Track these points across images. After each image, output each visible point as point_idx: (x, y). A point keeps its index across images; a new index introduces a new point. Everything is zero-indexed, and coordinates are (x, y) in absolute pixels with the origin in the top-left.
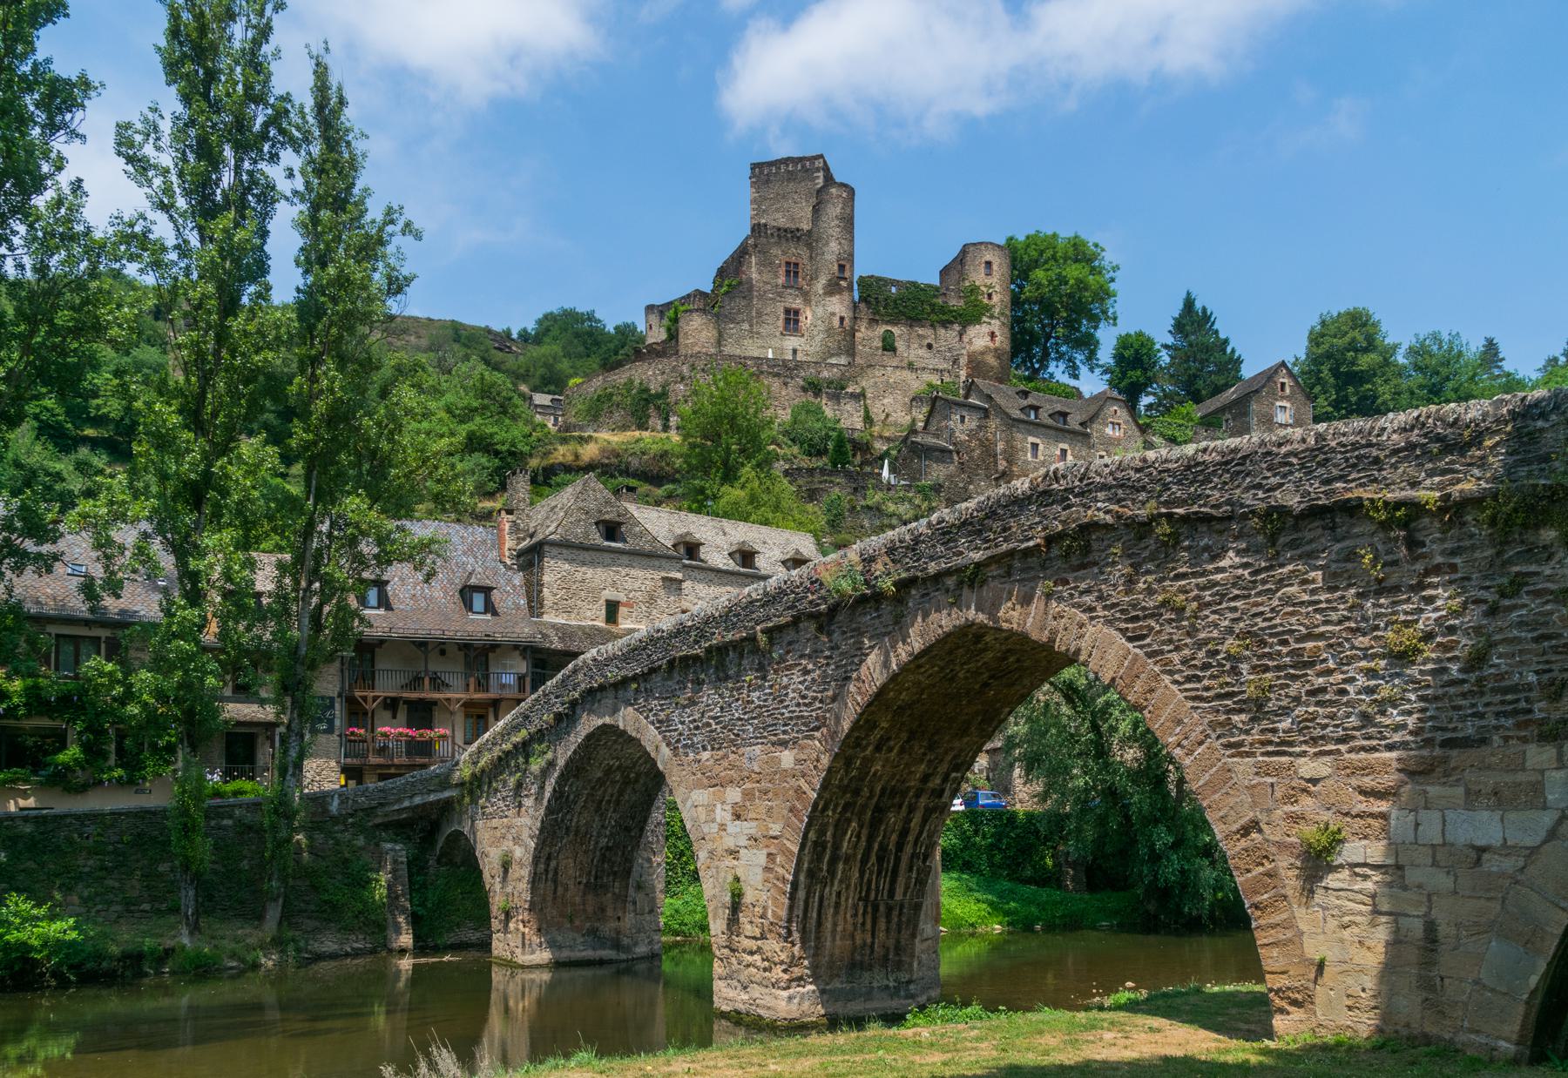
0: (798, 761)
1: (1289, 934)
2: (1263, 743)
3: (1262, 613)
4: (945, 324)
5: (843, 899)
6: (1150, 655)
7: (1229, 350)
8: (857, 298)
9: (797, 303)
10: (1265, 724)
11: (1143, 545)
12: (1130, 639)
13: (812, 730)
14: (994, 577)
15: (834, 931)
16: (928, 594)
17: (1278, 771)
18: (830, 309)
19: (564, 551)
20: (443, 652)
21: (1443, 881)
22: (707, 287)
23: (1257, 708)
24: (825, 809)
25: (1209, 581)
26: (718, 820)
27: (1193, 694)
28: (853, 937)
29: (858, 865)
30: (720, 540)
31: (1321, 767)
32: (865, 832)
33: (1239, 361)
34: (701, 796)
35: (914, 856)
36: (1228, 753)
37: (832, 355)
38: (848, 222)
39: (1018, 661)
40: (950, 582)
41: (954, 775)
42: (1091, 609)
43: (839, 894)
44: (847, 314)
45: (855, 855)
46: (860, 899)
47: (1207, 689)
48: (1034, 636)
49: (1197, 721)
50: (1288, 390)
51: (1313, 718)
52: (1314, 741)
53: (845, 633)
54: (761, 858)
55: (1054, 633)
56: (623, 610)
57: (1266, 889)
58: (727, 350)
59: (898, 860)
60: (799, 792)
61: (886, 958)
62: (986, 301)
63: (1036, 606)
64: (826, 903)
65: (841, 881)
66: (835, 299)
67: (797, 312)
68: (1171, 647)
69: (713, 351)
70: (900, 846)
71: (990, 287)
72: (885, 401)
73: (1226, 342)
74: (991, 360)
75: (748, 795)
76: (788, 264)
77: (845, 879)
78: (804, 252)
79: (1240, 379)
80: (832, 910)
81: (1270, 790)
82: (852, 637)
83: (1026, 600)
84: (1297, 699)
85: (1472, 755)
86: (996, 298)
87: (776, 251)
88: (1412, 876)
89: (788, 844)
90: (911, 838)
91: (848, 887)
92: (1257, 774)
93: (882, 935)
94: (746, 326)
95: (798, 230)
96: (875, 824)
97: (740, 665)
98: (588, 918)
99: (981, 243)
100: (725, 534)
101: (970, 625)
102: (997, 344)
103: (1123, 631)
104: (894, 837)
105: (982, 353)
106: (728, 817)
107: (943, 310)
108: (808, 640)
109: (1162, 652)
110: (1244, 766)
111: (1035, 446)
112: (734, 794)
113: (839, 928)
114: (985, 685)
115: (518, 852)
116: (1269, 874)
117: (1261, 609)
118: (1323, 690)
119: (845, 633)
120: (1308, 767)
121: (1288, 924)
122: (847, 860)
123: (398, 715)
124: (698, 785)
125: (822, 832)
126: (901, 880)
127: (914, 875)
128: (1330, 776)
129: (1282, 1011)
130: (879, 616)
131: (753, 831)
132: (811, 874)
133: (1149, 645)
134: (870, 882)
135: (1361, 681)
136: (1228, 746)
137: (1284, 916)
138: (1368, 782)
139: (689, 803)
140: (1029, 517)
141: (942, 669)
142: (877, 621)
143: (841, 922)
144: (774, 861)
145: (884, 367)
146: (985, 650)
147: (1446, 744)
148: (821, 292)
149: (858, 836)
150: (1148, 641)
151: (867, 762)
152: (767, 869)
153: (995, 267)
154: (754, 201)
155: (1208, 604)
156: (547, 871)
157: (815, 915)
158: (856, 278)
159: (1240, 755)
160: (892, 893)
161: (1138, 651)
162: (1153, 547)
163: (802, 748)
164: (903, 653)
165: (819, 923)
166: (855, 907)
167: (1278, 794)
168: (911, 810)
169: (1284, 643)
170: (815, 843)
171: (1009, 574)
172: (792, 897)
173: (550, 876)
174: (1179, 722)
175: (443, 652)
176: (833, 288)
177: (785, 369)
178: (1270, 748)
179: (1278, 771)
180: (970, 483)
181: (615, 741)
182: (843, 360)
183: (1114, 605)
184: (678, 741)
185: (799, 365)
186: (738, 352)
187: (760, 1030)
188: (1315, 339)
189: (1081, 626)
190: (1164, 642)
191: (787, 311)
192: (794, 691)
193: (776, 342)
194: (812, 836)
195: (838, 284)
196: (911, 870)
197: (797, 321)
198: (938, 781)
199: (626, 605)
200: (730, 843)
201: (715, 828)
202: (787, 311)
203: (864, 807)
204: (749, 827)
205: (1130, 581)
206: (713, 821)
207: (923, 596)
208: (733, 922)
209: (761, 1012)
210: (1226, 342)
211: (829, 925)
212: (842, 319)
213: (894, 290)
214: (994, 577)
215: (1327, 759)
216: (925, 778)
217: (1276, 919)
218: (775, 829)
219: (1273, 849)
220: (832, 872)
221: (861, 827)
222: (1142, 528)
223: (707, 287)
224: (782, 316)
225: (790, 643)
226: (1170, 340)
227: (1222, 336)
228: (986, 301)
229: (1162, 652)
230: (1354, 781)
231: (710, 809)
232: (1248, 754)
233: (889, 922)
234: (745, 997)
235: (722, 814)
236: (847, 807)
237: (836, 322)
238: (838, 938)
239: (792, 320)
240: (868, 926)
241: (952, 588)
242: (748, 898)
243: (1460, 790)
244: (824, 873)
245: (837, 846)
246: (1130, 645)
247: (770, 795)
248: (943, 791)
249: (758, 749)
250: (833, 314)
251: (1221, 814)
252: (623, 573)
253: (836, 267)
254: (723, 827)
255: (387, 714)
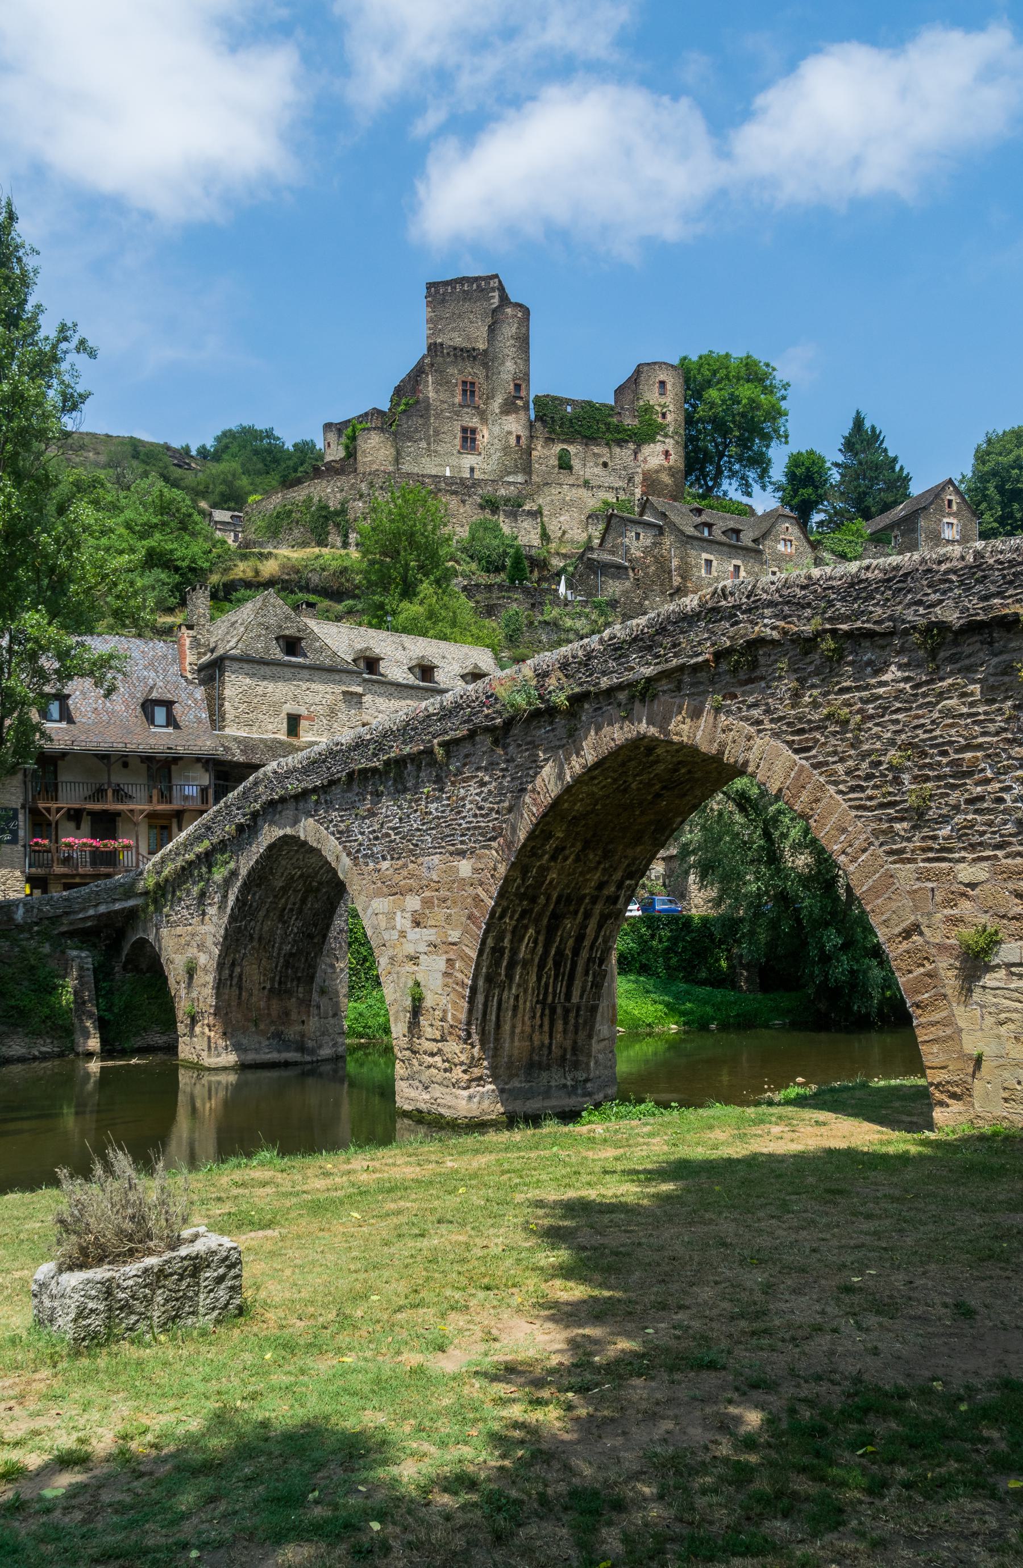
0: (476, 870)
1: (949, 1031)
2: (924, 850)
3: (923, 725)
4: (620, 443)
5: (521, 1002)
6: (815, 766)
7: (897, 468)
8: (533, 417)
9: (474, 422)
10: (926, 832)
11: (808, 660)
12: (796, 751)
13: (489, 840)
14: (664, 692)
15: (513, 1033)
16: (600, 708)
17: (938, 876)
18: (506, 428)
19: (245, 666)
20: (125, 765)
22: (386, 406)
23: (918, 817)
24: (502, 917)
25: (872, 695)
26: (398, 927)
27: (857, 803)
28: (531, 1039)
29: (535, 970)
30: (400, 655)
31: (979, 872)
32: (541, 938)
33: (907, 479)
34: (381, 904)
35: (590, 960)
36: (890, 859)
37: (509, 474)
38: (523, 342)
39: (689, 772)
40: (622, 696)
41: (628, 882)
42: (758, 722)
43: (517, 997)
44: (524, 433)
45: (532, 959)
46: (537, 1002)
47: (870, 798)
48: (704, 748)
49: (860, 829)
50: (955, 507)
51: (972, 826)
52: (973, 847)
53: (520, 746)
54: (440, 964)
55: (723, 745)
56: (304, 724)
57: (927, 988)
58: (405, 468)
59: (574, 965)
60: (477, 900)
61: (563, 1058)
62: (660, 420)
63: (705, 720)
64: (504, 1005)
65: (519, 986)
66: (511, 418)
67: (474, 431)
68: (836, 759)
69: (391, 468)
70: (576, 952)
71: (664, 406)
72: (562, 519)
73: (895, 460)
74: (666, 479)
75: (427, 903)
76: (464, 383)
77: (524, 982)
78: (480, 372)
79: (907, 496)
80: (510, 1013)
81: (930, 894)
82: (527, 750)
83: (696, 714)
84: (956, 808)
86: (670, 418)
87: (452, 370)
89: (467, 950)
90: (587, 943)
91: (525, 991)
92: (918, 879)
93: (558, 1037)
94: (423, 444)
95: (474, 349)
96: (551, 931)
97: (418, 777)
98: (273, 1022)
99: (655, 363)
100: (404, 649)
101: (641, 738)
102: (671, 463)
103: (791, 744)
104: (571, 942)
105: (657, 472)
106: (408, 924)
107: (618, 429)
108: (484, 753)
109: (827, 763)
110: (905, 872)
111: (709, 562)
112: (413, 902)
113: (518, 1030)
114: (658, 796)
115: (203, 959)
116: (929, 975)
117: (922, 721)
118: (981, 798)
119: (520, 746)
120: (966, 872)
121: (948, 1022)
122: (525, 964)
123: (83, 826)
124: (378, 894)
125: (500, 938)
126: (578, 984)
127: (590, 979)
128: (988, 880)
129: (942, 1104)
130: (553, 730)
131: (432, 938)
132: (489, 979)
133: (815, 757)
134: (547, 985)
136: (890, 853)
137: (944, 1014)
139: (370, 911)
140: (698, 633)
141: (615, 780)
142: (551, 734)
143: (519, 1025)
144: (453, 966)
145: (561, 485)
146: (657, 762)
148: (497, 411)
149: (536, 942)
150: (814, 752)
151: (544, 870)
152: (446, 974)
153: (669, 387)
154: (430, 321)
155: (871, 717)
156: (231, 976)
157: (494, 1018)
158: (532, 398)
159: (902, 861)
160: (568, 996)
161: (804, 762)
162: (818, 662)
163: (480, 857)
164: (576, 765)
165: (498, 1025)
166: (533, 1010)
167: (938, 899)
168: (587, 915)
169: (944, 753)
170: (494, 950)
171: (679, 689)
172: (471, 1001)
173: (235, 981)
174: (844, 830)
175: (125, 765)
176: (509, 407)
177: (463, 487)
178: (931, 855)
179: (938, 876)
180: (646, 598)
181: (297, 851)
182: (520, 478)
183: (781, 719)
184: (358, 851)
185: (476, 483)
186: (416, 470)
187: (442, 1128)
188: (981, 457)
189: (749, 738)
190: (829, 754)
191: (464, 430)
192: (471, 802)
193: (454, 461)
194: (490, 942)
195: (514, 403)
196: (587, 974)
197: (474, 440)
198: (613, 889)
199: (307, 718)
200: (410, 949)
201: (395, 935)
202: (464, 430)
203: (540, 915)
204: (429, 934)
205: (796, 695)
206: (394, 928)
207: (595, 710)
208: (414, 1025)
209: (442, 1111)
210: (895, 460)
211: (507, 1027)
212: (518, 438)
213: (569, 409)
214: (664, 692)
215: (985, 864)
216: (601, 886)
217: (936, 1016)
218: (454, 935)
219: (934, 951)
220: (510, 977)
221: (538, 933)
222: (808, 644)
223: (386, 406)
224: (459, 435)
225: (467, 756)
226: (840, 458)
227: (891, 454)
228: (660, 420)
229: (827, 763)
230: (1010, 885)
231: (391, 916)
232: (910, 861)
233: (566, 1023)
234: (427, 1097)
235: (402, 921)
236: (524, 913)
237: (513, 441)
238: (516, 1038)
239: (469, 439)
240: (546, 1028)
241: (624, 702)
242: (429, 1002)
244: (503, 977)
245: (514, 951)
246: (796, 757)
247: (449, 903)
248: (617, 898)
250: (510, 433)
251: (884, 918)
252: (304, 687)
253: (512, 387)
254: (403, 934)
255: (71, 825)
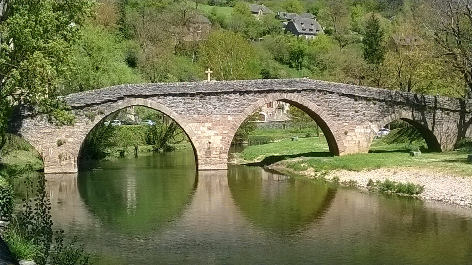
10: (339, 118)
17: (341, 124)
21: (360, 136)
31: (347, 124)
48: (299, 103)
54: (221, 138)
84: (343, 116)
85: (364, 123)
88: (357, 136)
103: (317, 104)
106: (205, 129)
112: (210, 125)
120: (345, 124)
121: (342, 142)
129: (341, 153)
135: (351, 114)
138: (352, 126)
147: (361, 122)
152: (221, 140)
163: (235, 116)
174: (326, 117)
179: (341, 124)
189: (309, 102)
217: (340, 142)
243: (362, 127)
247: (223, 125)
249: (218, 116)
